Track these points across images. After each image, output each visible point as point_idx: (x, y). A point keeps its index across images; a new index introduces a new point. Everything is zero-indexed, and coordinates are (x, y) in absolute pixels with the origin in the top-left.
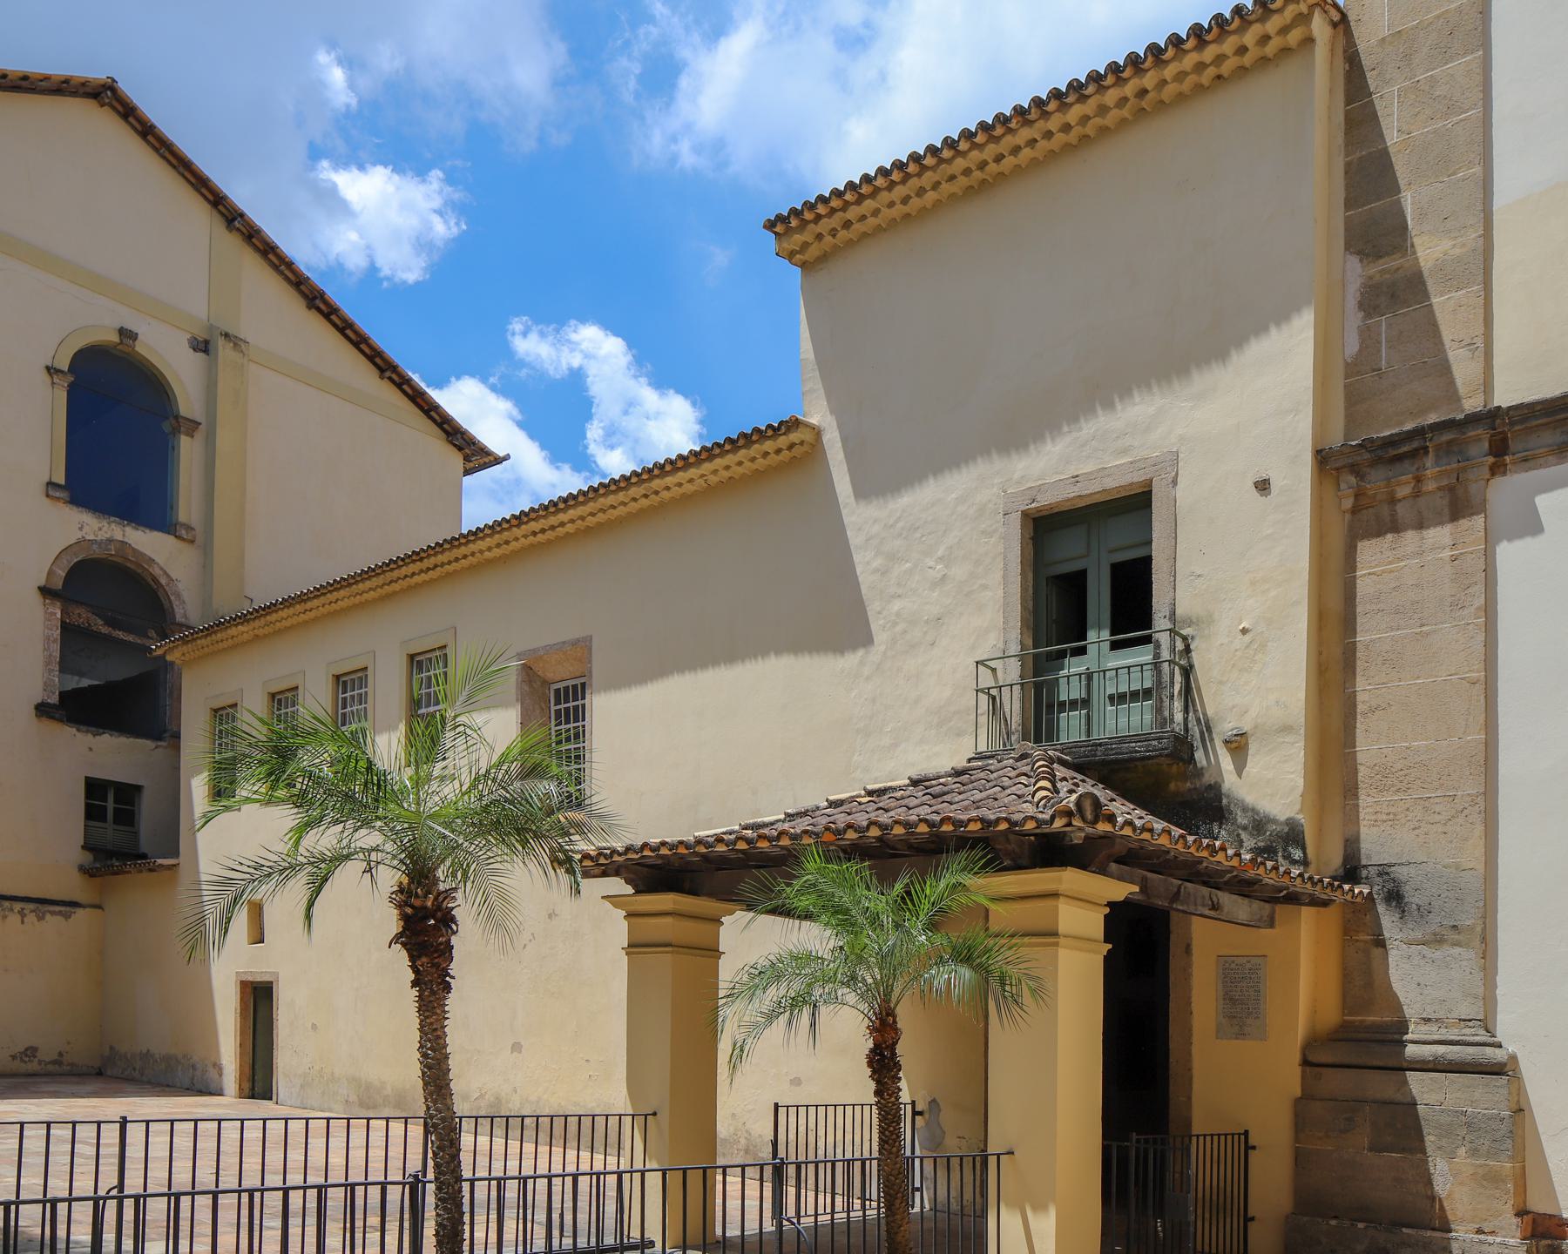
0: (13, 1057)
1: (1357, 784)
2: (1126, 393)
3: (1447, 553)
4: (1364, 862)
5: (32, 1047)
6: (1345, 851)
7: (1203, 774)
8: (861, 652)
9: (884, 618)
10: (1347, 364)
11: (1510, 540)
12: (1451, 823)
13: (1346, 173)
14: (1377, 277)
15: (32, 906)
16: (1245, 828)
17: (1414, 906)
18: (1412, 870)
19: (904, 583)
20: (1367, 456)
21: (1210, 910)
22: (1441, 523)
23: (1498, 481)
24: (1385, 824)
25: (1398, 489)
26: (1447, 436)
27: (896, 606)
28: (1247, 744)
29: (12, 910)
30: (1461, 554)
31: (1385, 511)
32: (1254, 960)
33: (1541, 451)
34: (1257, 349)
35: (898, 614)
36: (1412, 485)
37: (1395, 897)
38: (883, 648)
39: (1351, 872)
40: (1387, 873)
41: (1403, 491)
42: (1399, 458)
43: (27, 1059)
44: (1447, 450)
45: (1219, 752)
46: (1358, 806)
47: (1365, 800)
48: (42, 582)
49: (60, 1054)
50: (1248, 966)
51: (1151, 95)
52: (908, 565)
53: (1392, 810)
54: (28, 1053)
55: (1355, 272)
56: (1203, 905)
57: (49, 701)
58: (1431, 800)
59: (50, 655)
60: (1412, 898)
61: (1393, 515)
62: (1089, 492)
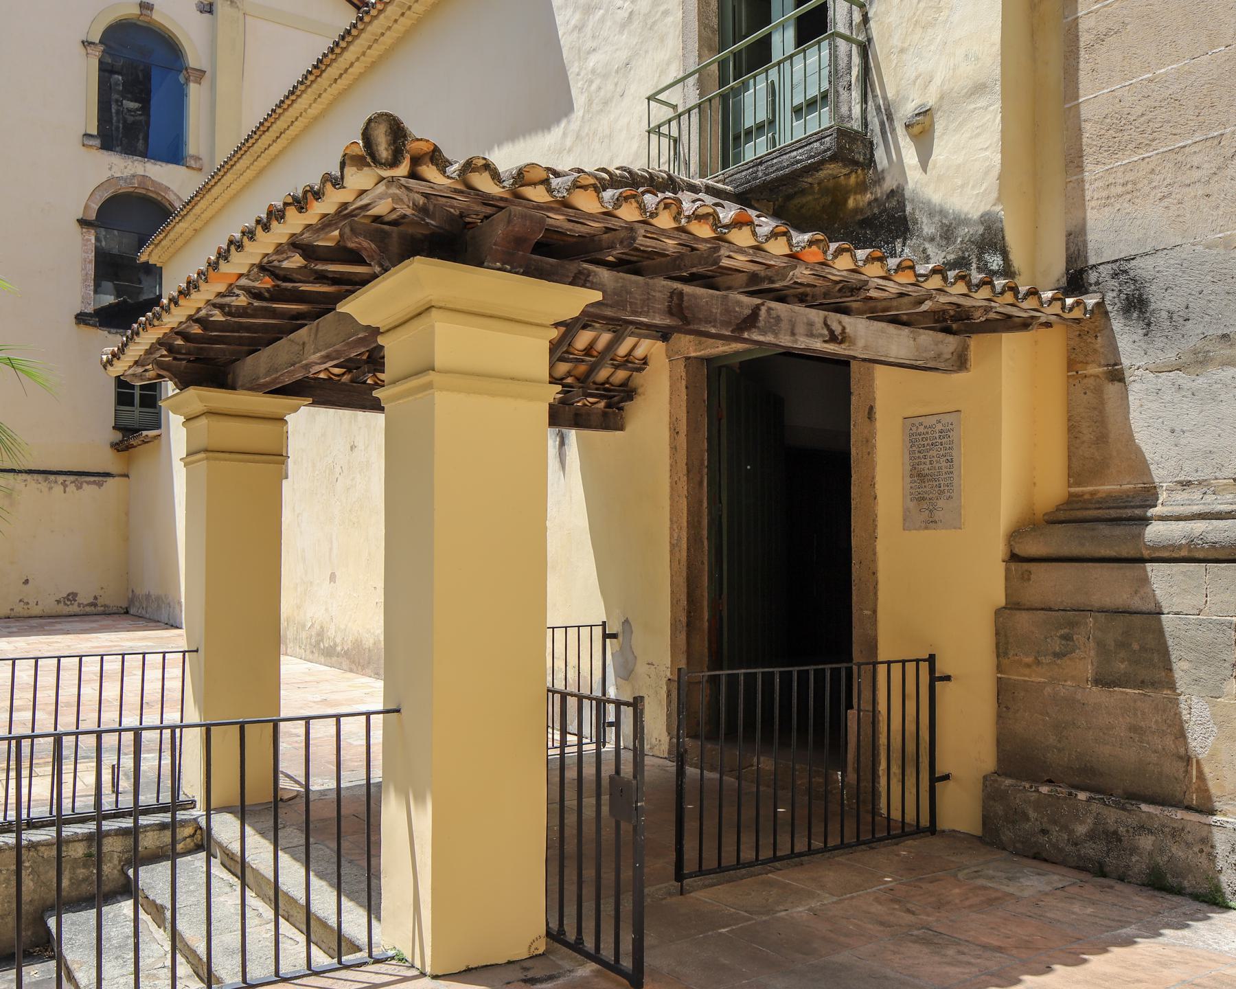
0: (58, 602)
1: (1081, 150)
4: (1092, 261)
5: (72, 593)
6: (1067, 249)
7: (883, 178)
9: (583, 79)
12: (1216, 178)
15: (72, 478)
16: (932, 239)
17: (1164, 314)
18: (1160, 260)
21: (825, 342)
24: (1121, 200)
27: (592, 61)
28: (932, 124)
29: (56, 482)
32: (947, 419)
35: (593, 71)
37: (1136, 305)
38: (580, 113)
39: (1076, 282)
40: (1125, 272)
43: (69, 603)
45: (902, 144)
46: (1083, 181)
47: (1092, 171)
48: (80, 216)
49: (96, 598)
50: (939, 427)
52: (602, 12)
53: (1130, 176)
54: (70, 597)
56: (811, 335)
57: (86, 311)
58: (1187, 149)
59: (87, 274)
60: (1160, 302)
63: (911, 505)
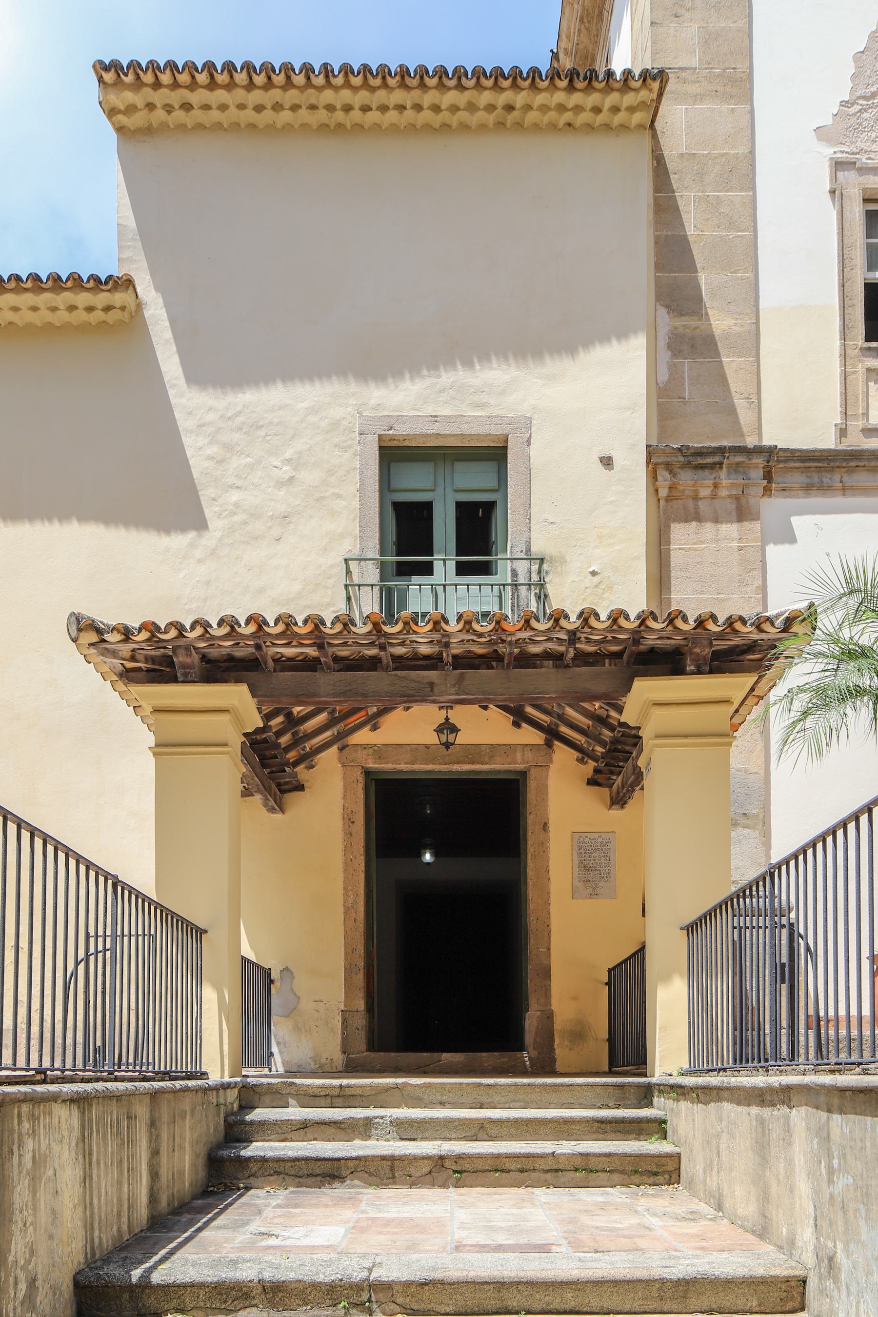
2: (485, 358)
3: (735, 544)
8: (192, 535)
10: (659, 388)
11: (775, 544)
13: (656, 243)
14: (681, 330)
19: (244, 476)
20: (682, 459)
22: (731, 522)
23: (766, 500)
25: (701, 490)
26: (739, 459)
30: (745, 546)
31: (690, 504)
32: (605, 836)
33: (796, 485)
34: (600, 353)
36: (711, 489)
41: (705, 492)
42: (702, 467)
44: (737, 468)
50: (600, 840)
51: (515, 113)
55: (665, 320)
61: (696, 508)
62: (447, 432)
63: (579, 885)
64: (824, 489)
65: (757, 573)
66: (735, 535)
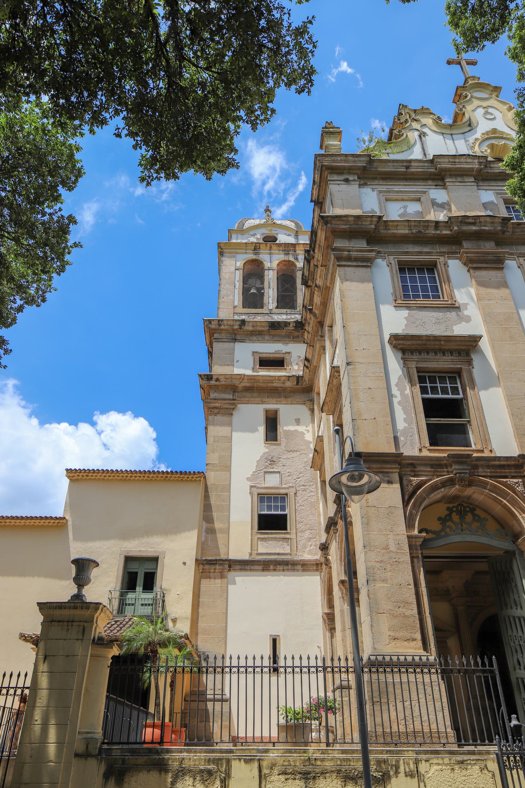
64: (245, 570)
65: (225, 594)
66: (220, 582)
